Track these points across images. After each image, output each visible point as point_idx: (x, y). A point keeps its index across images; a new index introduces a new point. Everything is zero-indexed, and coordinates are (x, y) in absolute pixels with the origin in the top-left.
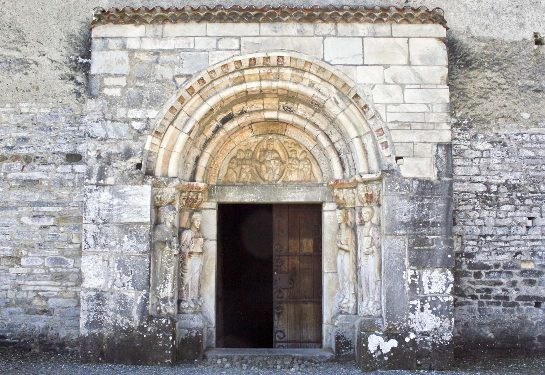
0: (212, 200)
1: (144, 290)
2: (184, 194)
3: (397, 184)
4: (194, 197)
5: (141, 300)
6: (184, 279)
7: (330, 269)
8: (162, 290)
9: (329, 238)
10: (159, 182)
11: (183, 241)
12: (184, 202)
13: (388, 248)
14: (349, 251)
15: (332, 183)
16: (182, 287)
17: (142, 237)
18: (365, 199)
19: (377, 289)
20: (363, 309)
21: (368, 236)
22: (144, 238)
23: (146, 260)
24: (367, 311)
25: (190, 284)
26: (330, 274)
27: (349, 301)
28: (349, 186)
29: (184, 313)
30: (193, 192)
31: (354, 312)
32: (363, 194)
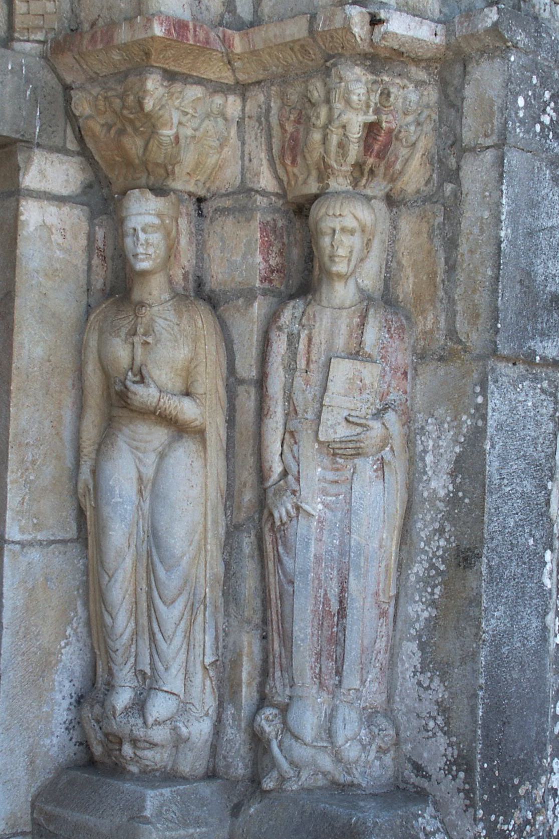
3: (547, 95)
7: (37, 527)
9: (39, 351)
13: (500, 428)
14: (200, 434)
15: (158, 30)
18: (354, 151)
19: (381, 644)
20: (301, 752)
21: (357, 354)
24: (326, 762)
26: (35, 555)
27: (184, 707)
28: (216, 71)
31: (200, 767)
32: (356, 122)
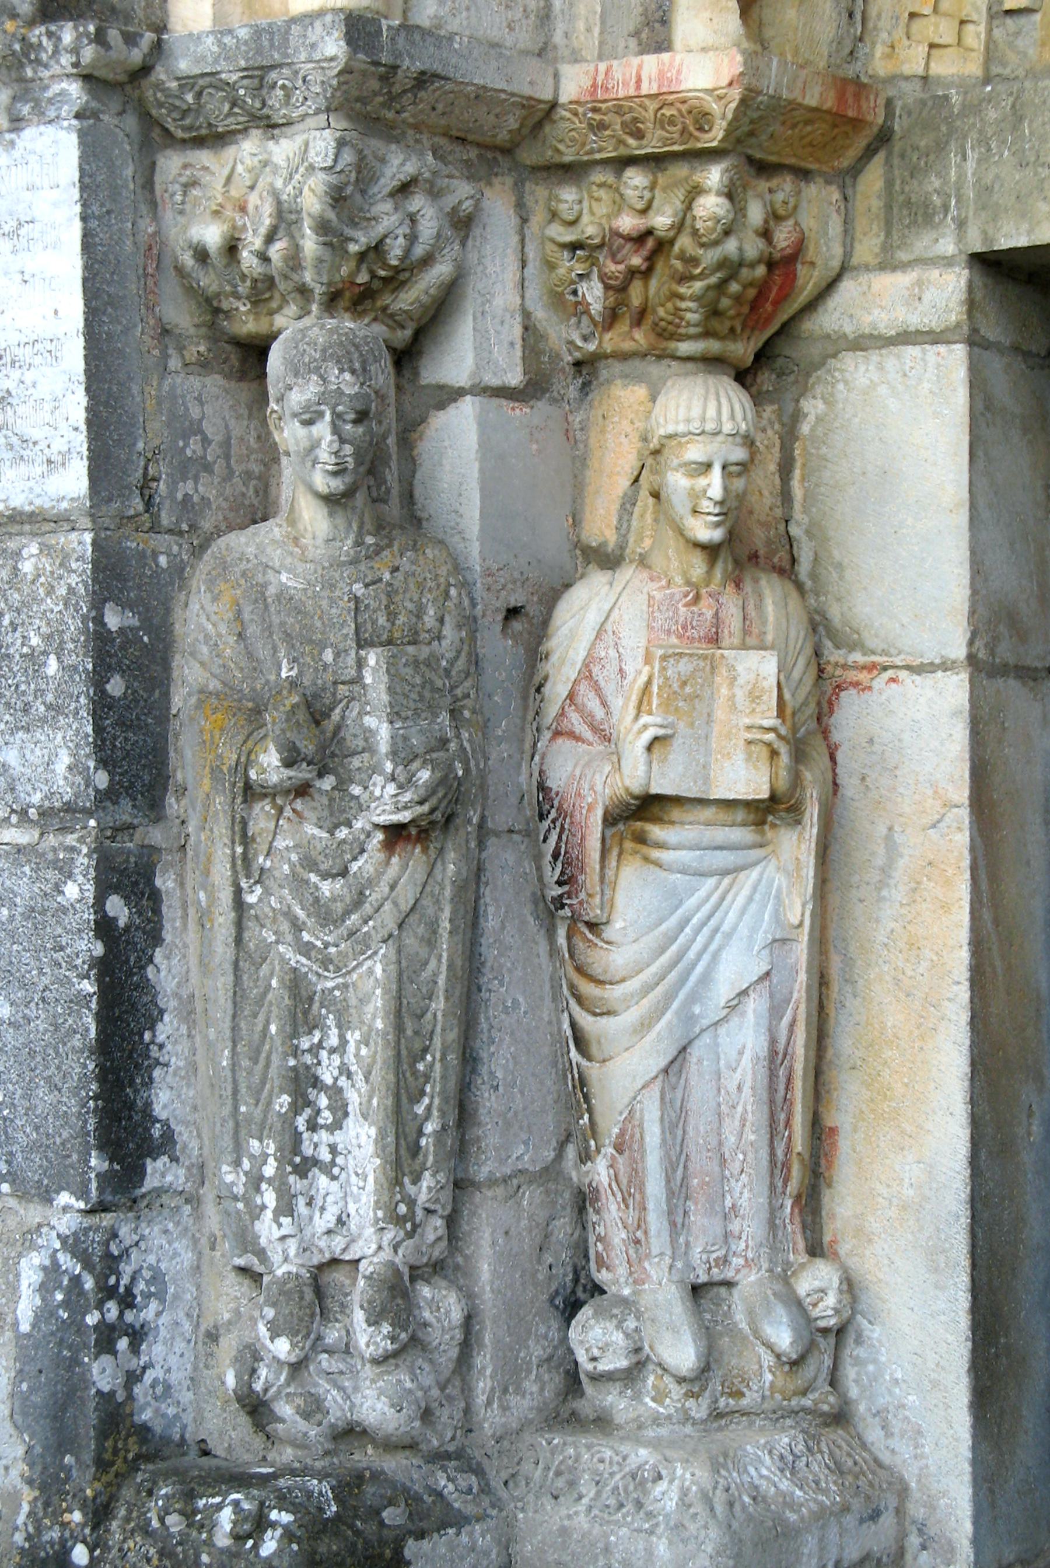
0: (923, 243)
1: (65, 1198)
2: (568, 195)
4: (662, 221)
5: (44, 1289)
6: (593, 1070)
8: (269, 1197)
10: (187, 82)
11: (557, 690)
12: (593, 293)
16: (585, 1157)
17: (34, 659)
22: (52, 666)
23: (72, 891)
25: (653, 1135)
29: (602, 1423)
30: (656, 161)
